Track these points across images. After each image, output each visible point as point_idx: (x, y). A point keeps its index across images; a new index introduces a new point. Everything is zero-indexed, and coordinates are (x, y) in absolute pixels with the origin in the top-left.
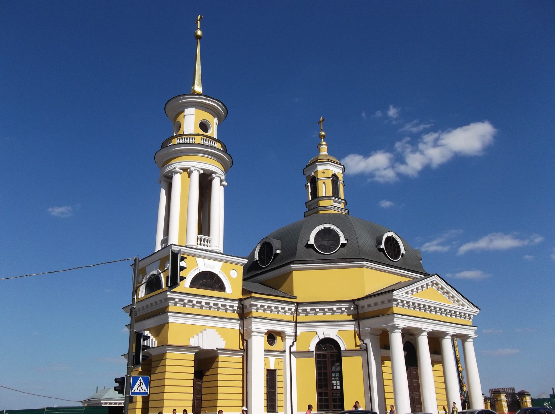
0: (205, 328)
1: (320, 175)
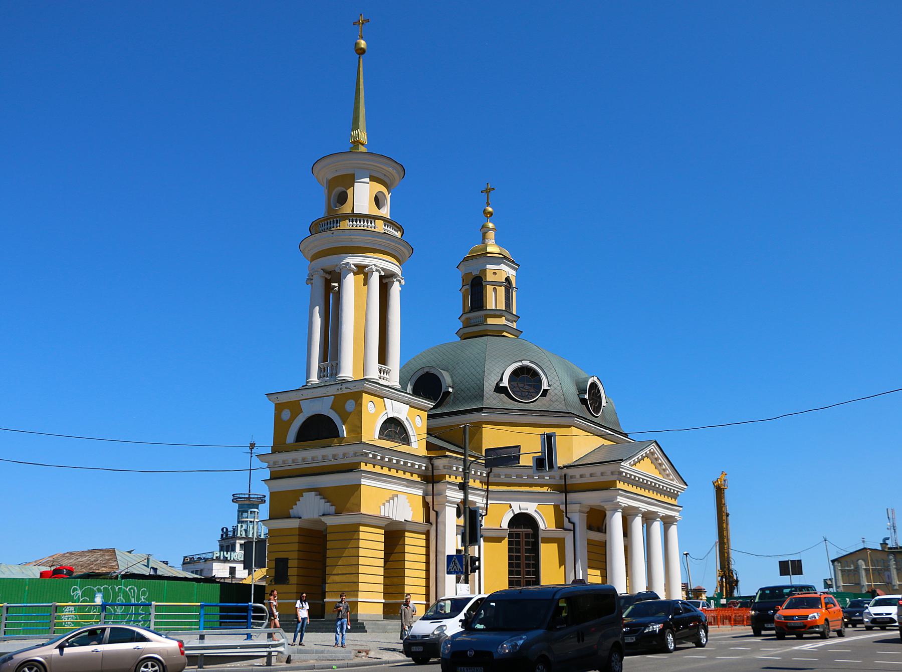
1: (490, 277)
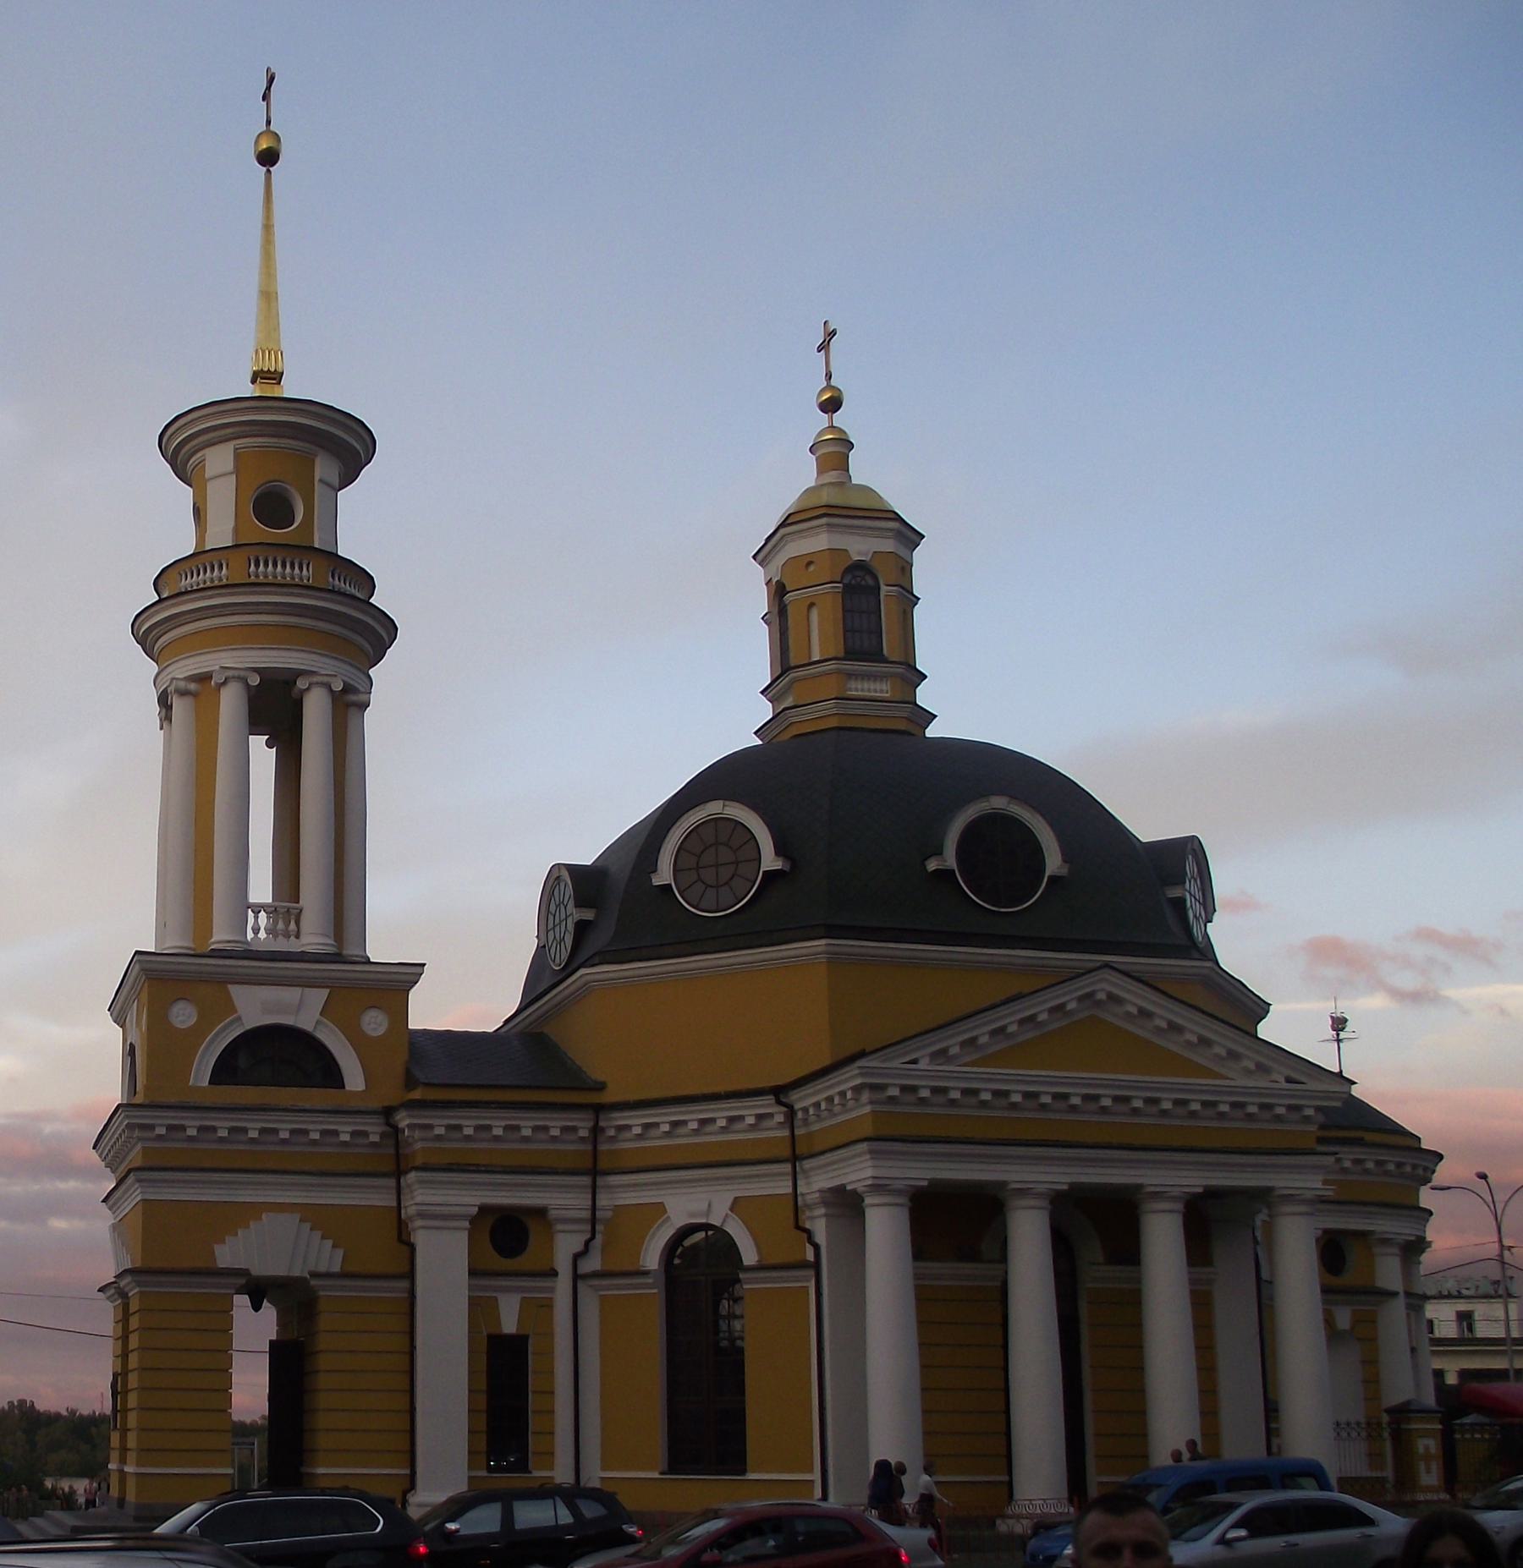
0: (253, 1211)
